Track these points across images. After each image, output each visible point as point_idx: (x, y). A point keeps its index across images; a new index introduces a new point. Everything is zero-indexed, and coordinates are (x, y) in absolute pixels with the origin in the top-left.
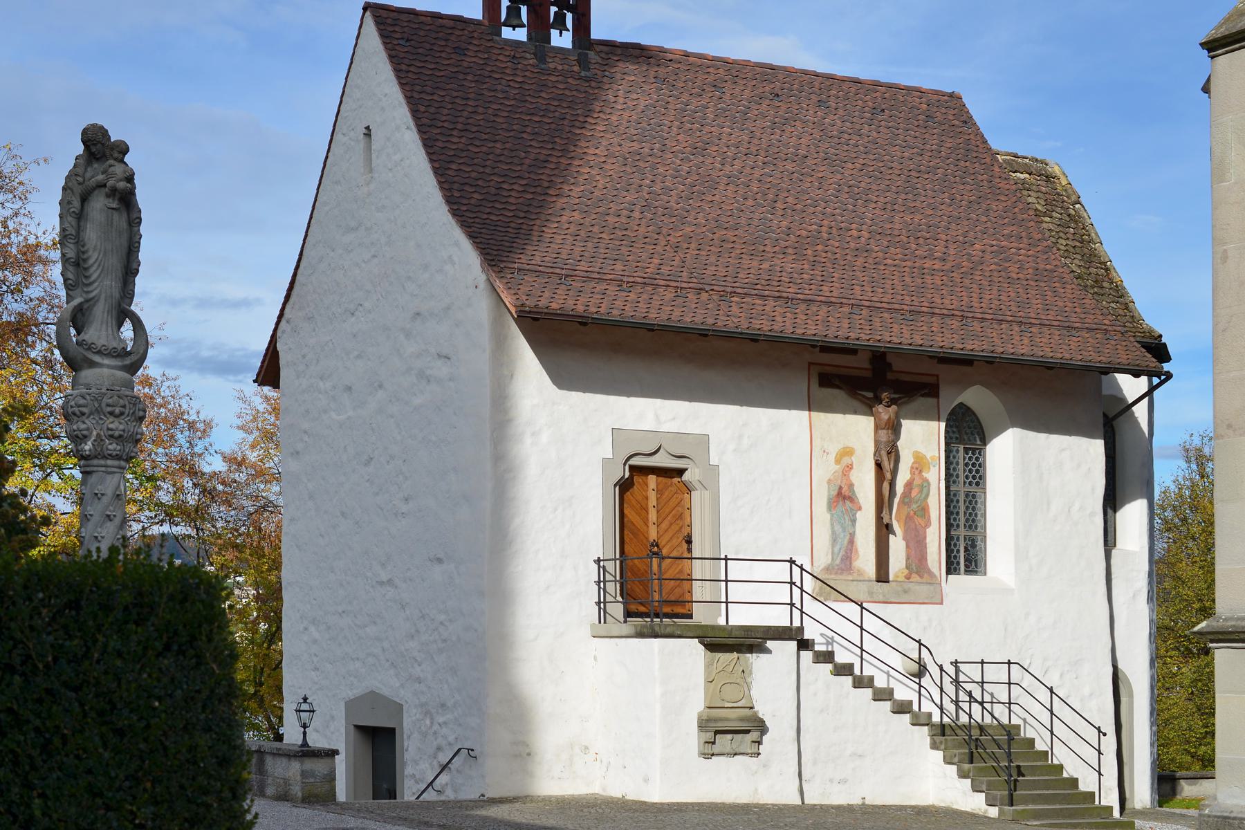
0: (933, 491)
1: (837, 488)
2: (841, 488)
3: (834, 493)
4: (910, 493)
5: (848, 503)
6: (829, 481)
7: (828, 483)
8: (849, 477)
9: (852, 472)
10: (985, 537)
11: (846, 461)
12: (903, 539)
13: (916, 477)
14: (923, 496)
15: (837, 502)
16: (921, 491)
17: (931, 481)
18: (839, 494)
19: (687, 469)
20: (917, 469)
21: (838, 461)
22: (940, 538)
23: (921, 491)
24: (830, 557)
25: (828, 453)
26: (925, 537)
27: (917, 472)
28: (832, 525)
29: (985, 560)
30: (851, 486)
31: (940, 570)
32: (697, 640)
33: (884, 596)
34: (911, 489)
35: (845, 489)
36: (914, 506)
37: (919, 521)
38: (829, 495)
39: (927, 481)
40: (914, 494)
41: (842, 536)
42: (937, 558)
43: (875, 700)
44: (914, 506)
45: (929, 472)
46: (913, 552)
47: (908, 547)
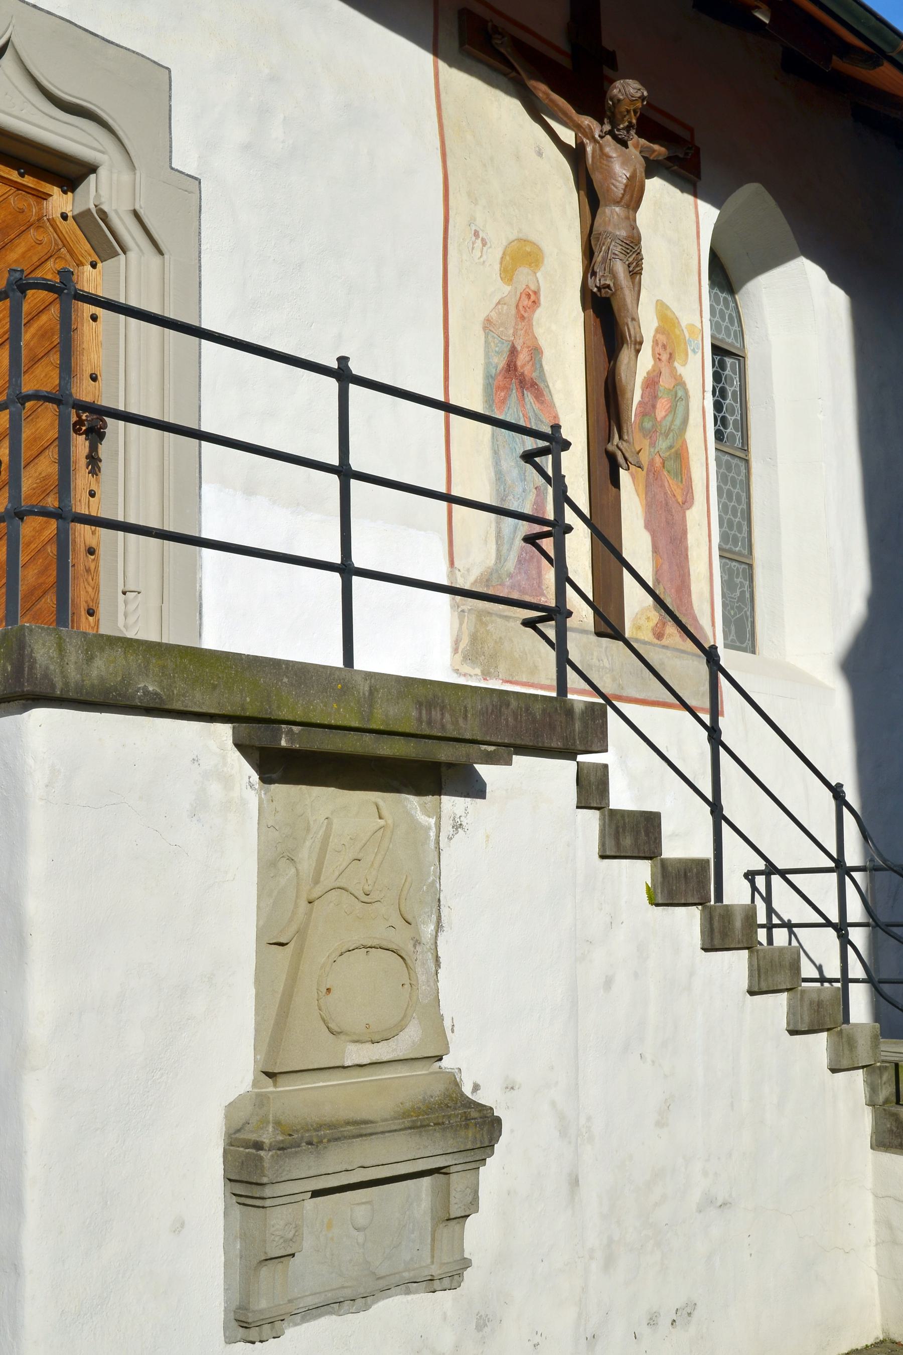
0: (695, 417)
1: (506, 349)
2: (513, 351)
3: (500, 362)
4: (654, 407)
5: (529, 397)
6: (488, 325)
7: (485, 328)
8: (530, 325)
9: (538, 311)
10: (751, 566)
11: (523, 276)
12: (648, 526)
13: (665, 371)
14: (678, 422)
15: (506, 388)
16: (673, 409)
17: (691, 393)
18: (511, 367)
19: (92, 169)
20: (664, 347)
21: (507, 273)
22: (710, 541)
23: (673, 409)
24: (494, 547)
25: (484, 243)
26: (685, 532)
27: (665, 357)
28: (496, 453)
29: (753, 623)
30: (536, 352)
31: (713, 625)
32: (225, 731)
33: (614, 679)
34: (655, 397)
35: (522, 358)
36: (662, 444)
37: (671, 483)
38: (488, 365)
39: (680, 383)
40: (660, 413)
41: (519, 489)
42: (707, 594)
43: (752, 993)
44: (662, 444)
45: (685, 363)
46: (666, 567)
47: (655, 549)
